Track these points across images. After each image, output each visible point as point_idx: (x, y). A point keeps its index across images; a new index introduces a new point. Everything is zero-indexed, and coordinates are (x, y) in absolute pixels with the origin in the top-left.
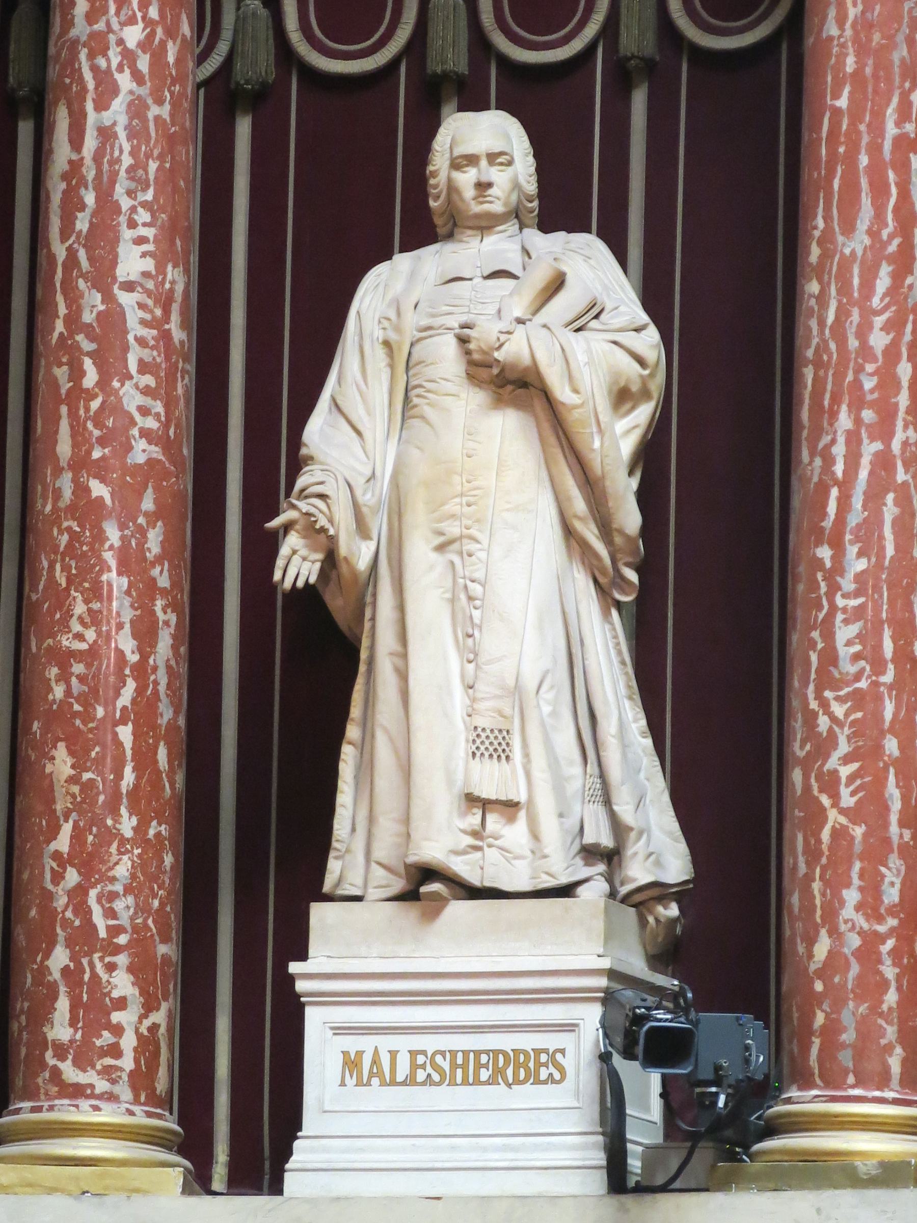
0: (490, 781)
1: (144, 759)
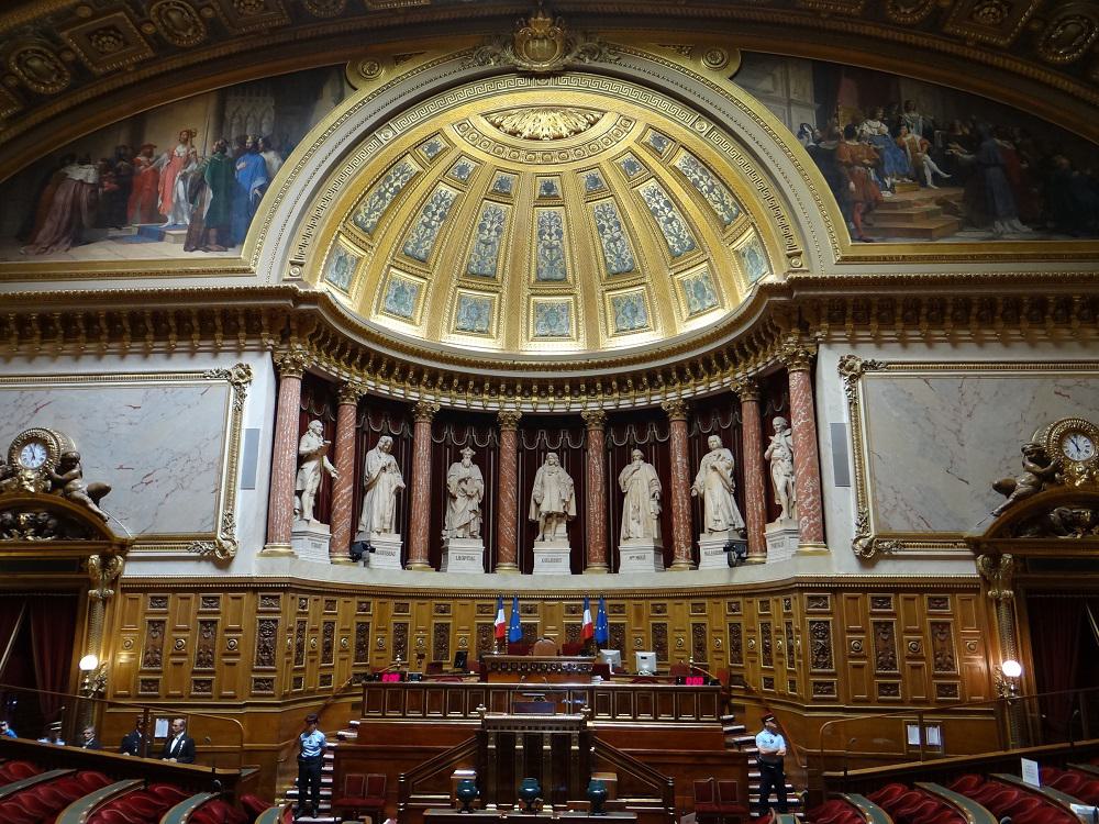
1: (684, 518)
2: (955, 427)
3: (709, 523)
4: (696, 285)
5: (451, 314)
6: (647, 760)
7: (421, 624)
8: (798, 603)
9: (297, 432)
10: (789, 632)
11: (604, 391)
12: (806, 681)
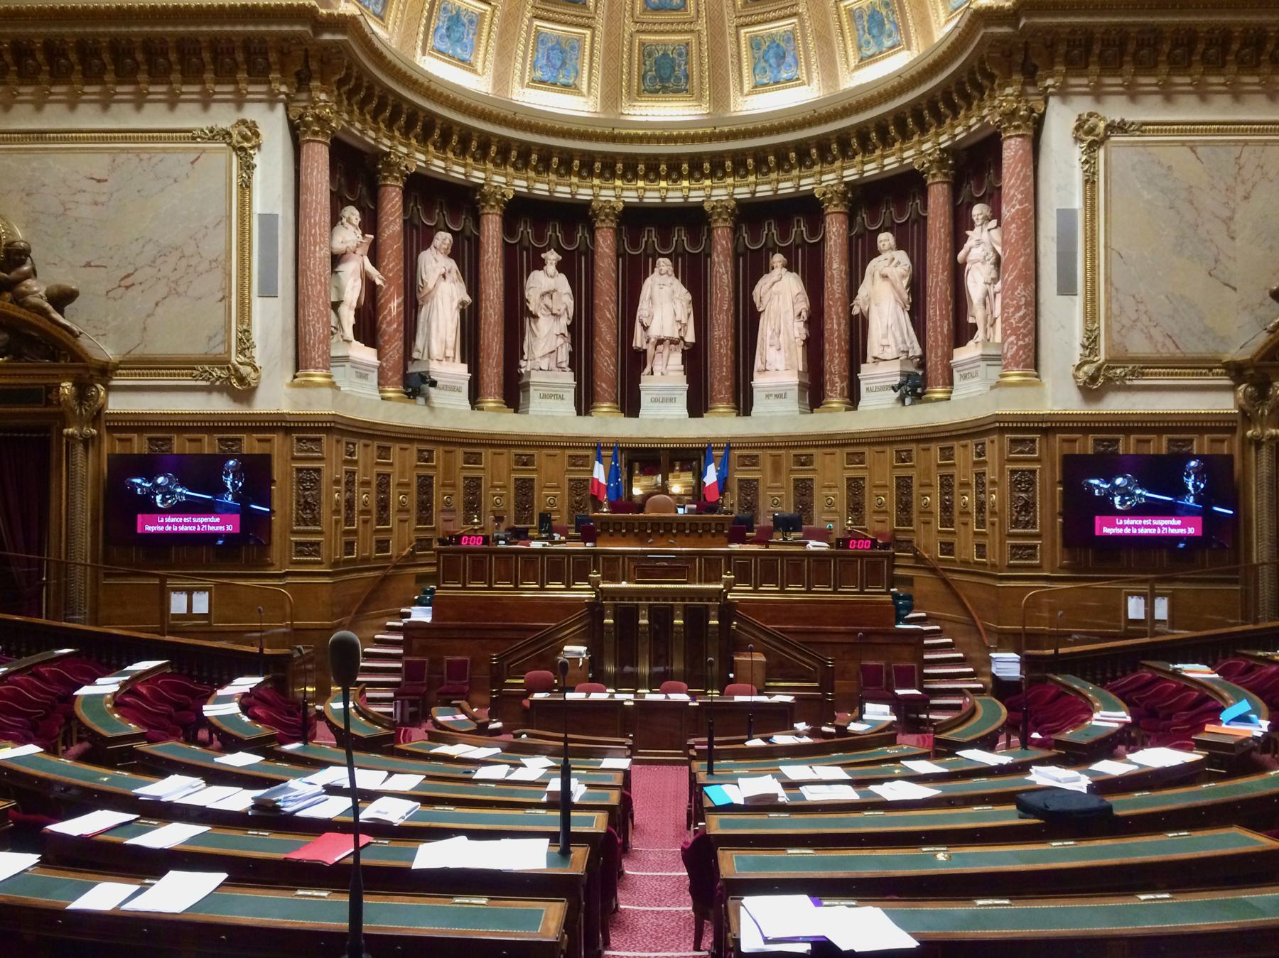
0: (884, 342)
1: (839, 344)
2: (1227, 213)
3: (874, 348)
4: (871, 16)
5: (524, 59)
6: (805, 638)
7: (498, 479)
8: (994, 448)
9: (328, 219)
10: (980, 485)
11: (735, 173)
12: (1002, 543)
